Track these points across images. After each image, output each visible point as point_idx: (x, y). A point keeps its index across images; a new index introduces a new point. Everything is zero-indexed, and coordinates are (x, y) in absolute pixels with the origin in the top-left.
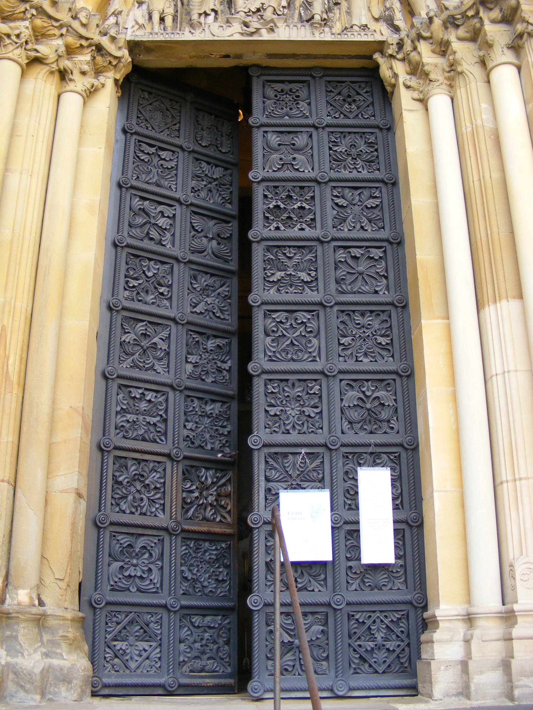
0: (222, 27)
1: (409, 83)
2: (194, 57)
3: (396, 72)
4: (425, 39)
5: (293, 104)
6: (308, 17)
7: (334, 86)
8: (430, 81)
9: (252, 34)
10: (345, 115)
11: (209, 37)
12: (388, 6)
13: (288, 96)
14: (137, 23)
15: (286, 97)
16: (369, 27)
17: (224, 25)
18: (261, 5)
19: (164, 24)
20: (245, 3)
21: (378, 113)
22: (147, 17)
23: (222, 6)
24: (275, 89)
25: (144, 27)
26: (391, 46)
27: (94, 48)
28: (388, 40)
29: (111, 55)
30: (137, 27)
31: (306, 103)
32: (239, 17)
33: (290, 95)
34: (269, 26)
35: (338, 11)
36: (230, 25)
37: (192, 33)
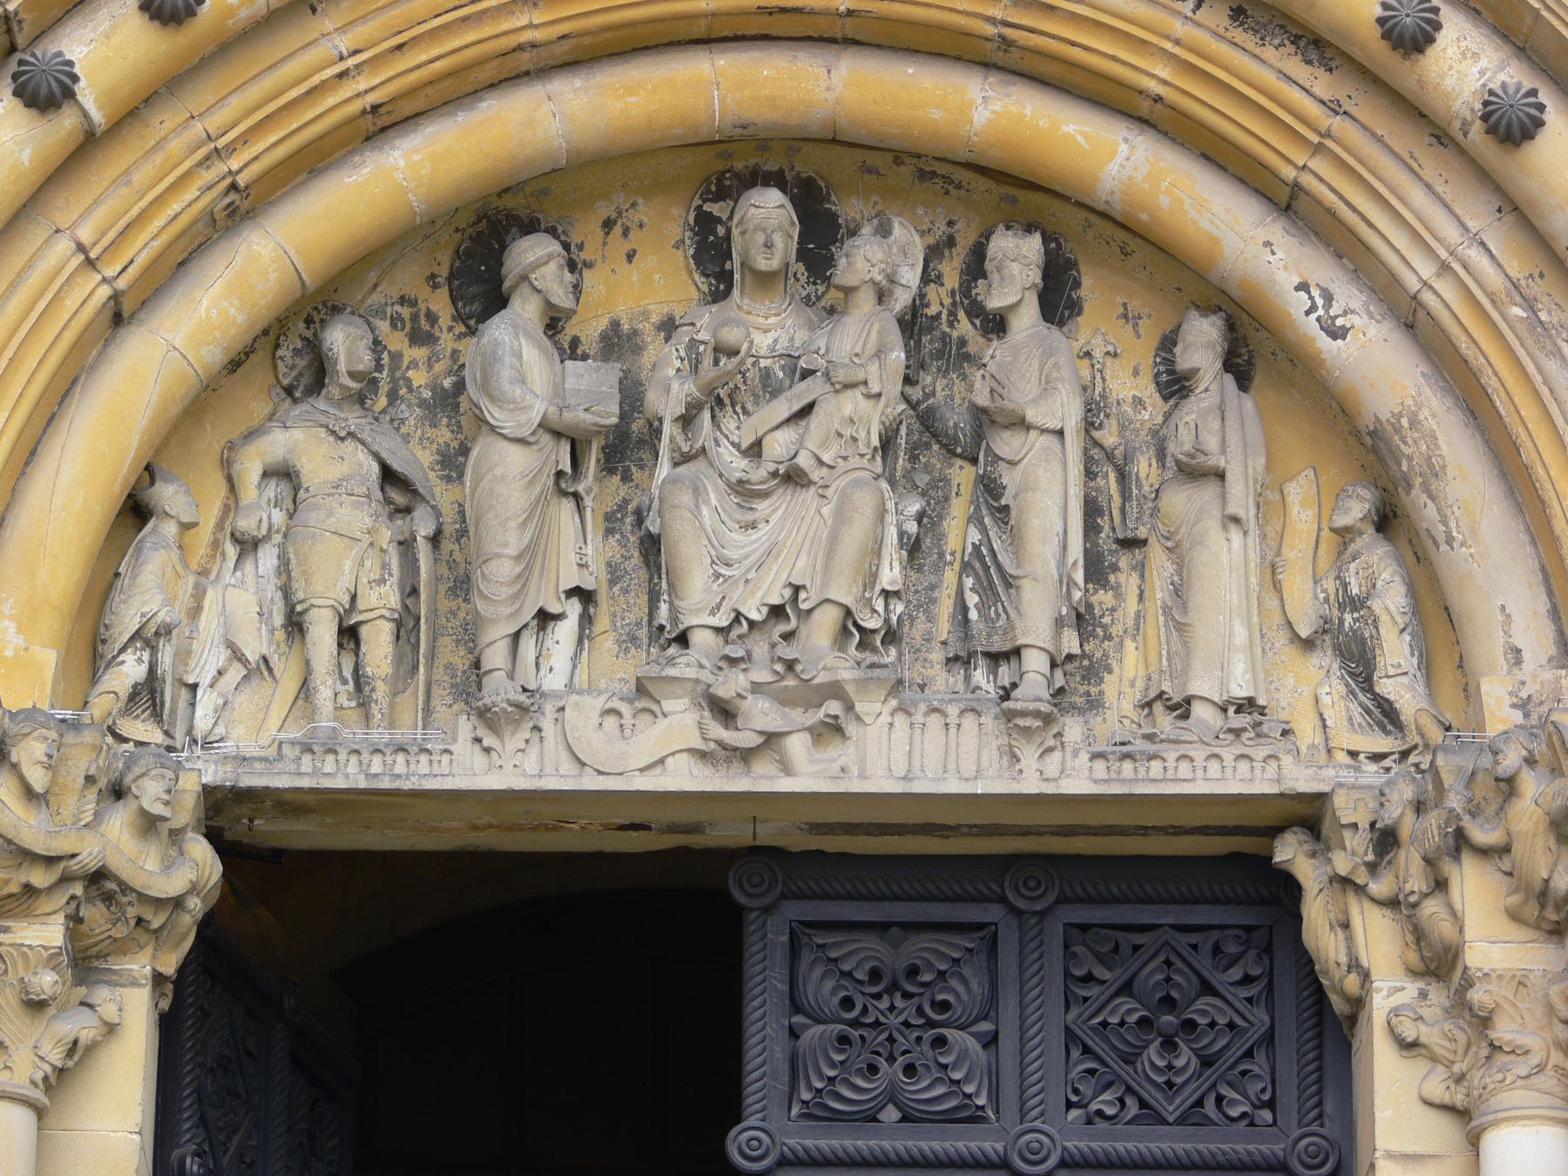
0: (617, 713)
1: (1410, 1033)
2: (490, 826)
3: (1365, 963)
4: (1484, 852)
5: (919, 1039)
6: (998, 645)
7: (1105, 948)
8: (1495, 1048)
9: (746, 756)
10: (1143, 1104)
11: (560, 777)
12: (1355, 590)
13: (899, 1002)
14: (237, 655)
15: (892, 1008)
16: (1261, 702)
17: (625, 709)
18: (788, 593)
19: (357, 653)
20: (717, 576)
21: (1288, 1097)
22: (278, 620)
23: (612, 541)
24: (846, 967)
25: (270, 670)
26: (1347, 834)
27: (78, 889)
28: (1339, 801)
29: (143, 898)
30: (236, 673)
31: (975, 1035)
32: (691, 673)
33: (907, 996)
34: (821, 714)
35: (1134, 579)
36: (654, 707)
37: (487, 750)
